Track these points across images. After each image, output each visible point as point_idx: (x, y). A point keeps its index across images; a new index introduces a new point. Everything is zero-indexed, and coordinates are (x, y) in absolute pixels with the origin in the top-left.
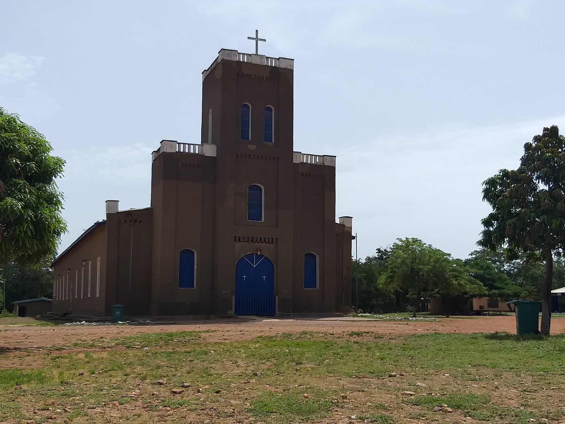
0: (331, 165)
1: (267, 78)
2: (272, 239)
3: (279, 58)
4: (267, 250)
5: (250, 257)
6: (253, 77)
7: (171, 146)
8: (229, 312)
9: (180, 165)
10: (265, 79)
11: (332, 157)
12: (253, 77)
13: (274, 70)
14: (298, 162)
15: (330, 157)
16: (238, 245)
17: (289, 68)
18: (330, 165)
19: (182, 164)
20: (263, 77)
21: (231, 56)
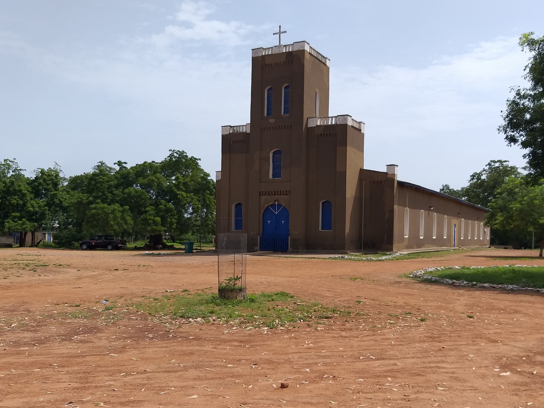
0: (343, 123)
1: (283, 62)
2: (278, 191)
3: (294, 43)
4: (283, 200)
5: (273, 206)
6: (273, 65)
7: (226, 130)
8: (256, 248)
9: (231, 143)
10: (282, 64)
11: (344, 116)
12: (273, 65)
13: (289, 55)
14: (314, 125)
15: (342, 116)
16: (263, 197)
17: (301, 49)
18: (342, 123)
19: (233, 141)
20: (281, 63)
21: (258, 53)
